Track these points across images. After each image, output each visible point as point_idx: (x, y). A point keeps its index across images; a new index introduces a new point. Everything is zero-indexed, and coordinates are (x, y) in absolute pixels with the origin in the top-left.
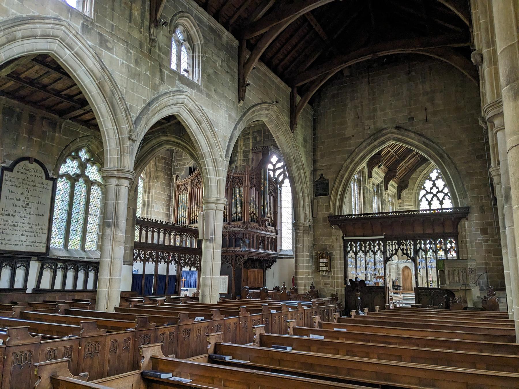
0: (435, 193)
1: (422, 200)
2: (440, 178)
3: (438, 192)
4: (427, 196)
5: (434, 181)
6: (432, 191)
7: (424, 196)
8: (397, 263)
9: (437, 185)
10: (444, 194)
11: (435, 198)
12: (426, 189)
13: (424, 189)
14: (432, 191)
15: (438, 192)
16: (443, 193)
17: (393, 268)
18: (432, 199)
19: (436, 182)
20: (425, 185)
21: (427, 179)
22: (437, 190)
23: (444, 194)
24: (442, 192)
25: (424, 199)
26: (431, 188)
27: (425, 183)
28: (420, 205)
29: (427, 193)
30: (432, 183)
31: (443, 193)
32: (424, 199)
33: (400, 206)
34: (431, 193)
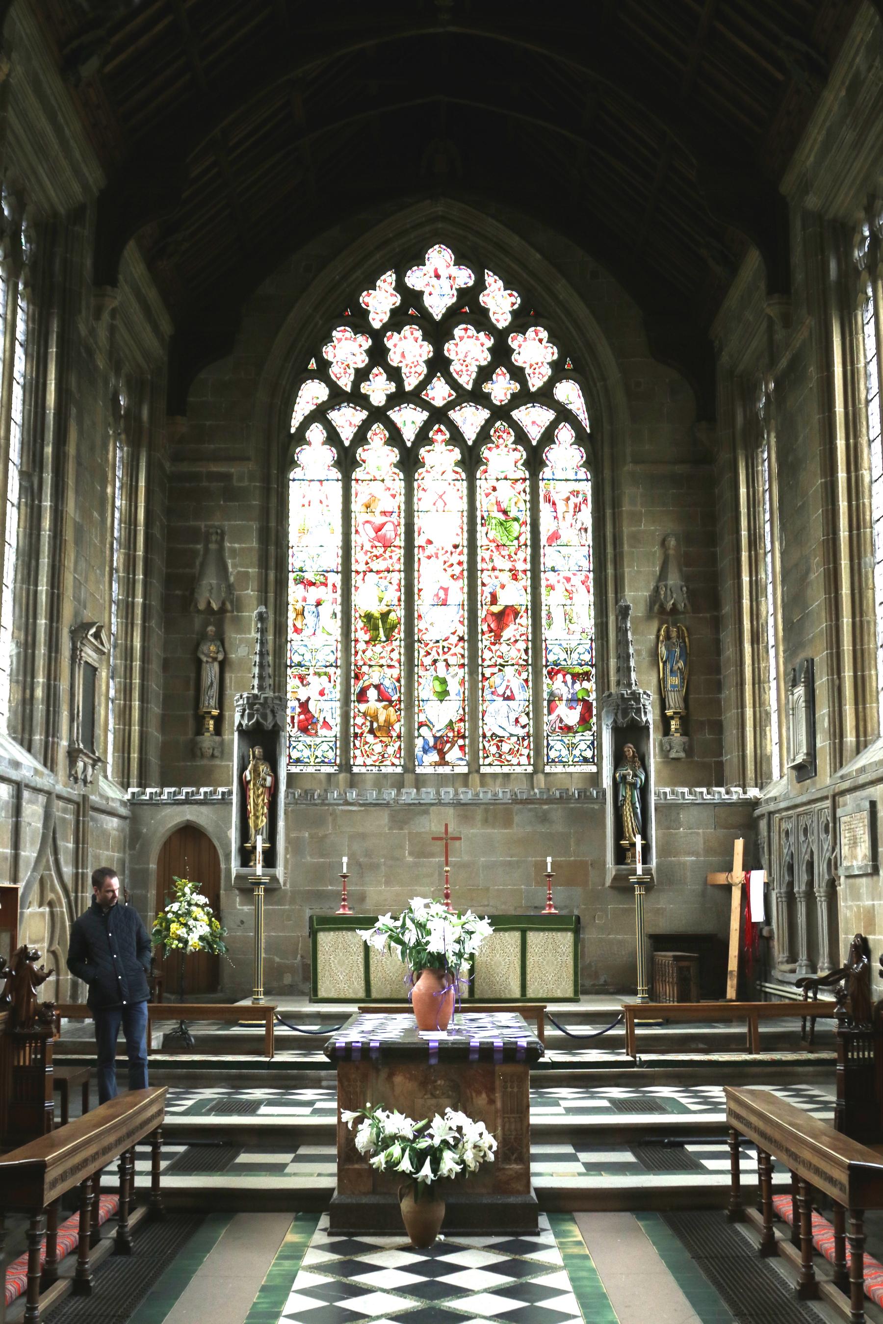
0: (378, 399)
1: (308, 435)
2: (412, 321)
3: (398, 398)
4: (334, 416)
5: (377, 336)
6: (365, 388)
7: (319, 414)
8: (134, 803)
9: (394, 359)
10: (425, 415)
11: (378, 434)
12: (334, 371)
13: (323, 372)
14: (365, 388)
15: (398, 398)
16: (425, 405)
17: (105, 833)
18: (361, 437)
19: (392, 341)
20: (328, 352)
21: (337, 320)
22: (392, 387)
23: (425, 415)
24: (416, 397)
25: (316, 433)
26: (362, 375)
27: (328, 339)
28: (292, 463)
29: (337, 397)
30: (367, 343)
31: (425, 405)
32: (316, 433)
33: (176, 458)
34: (358, 398)
